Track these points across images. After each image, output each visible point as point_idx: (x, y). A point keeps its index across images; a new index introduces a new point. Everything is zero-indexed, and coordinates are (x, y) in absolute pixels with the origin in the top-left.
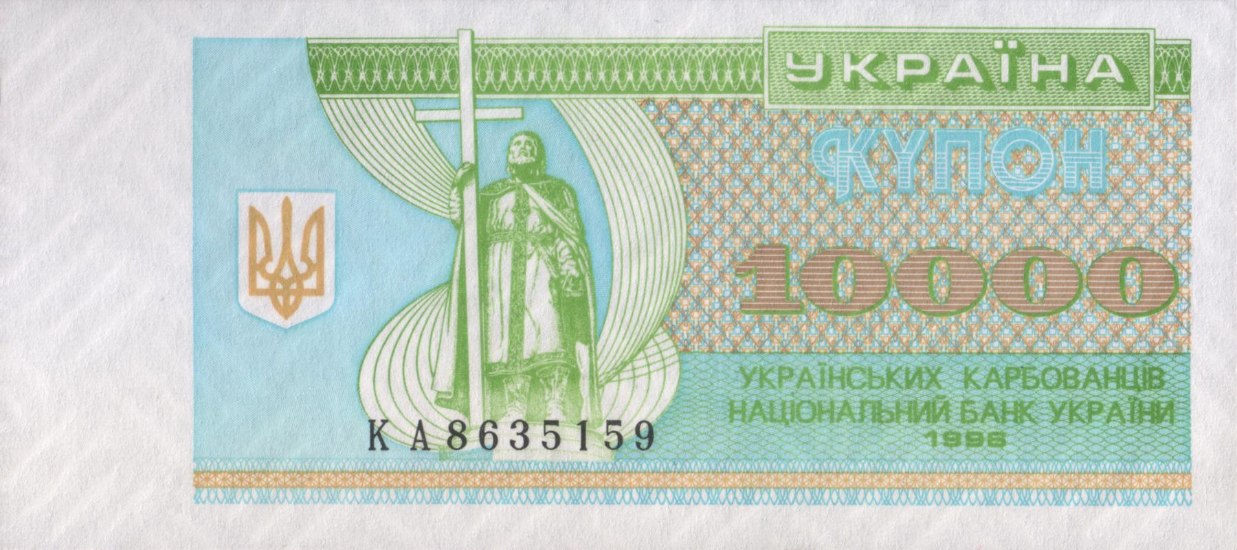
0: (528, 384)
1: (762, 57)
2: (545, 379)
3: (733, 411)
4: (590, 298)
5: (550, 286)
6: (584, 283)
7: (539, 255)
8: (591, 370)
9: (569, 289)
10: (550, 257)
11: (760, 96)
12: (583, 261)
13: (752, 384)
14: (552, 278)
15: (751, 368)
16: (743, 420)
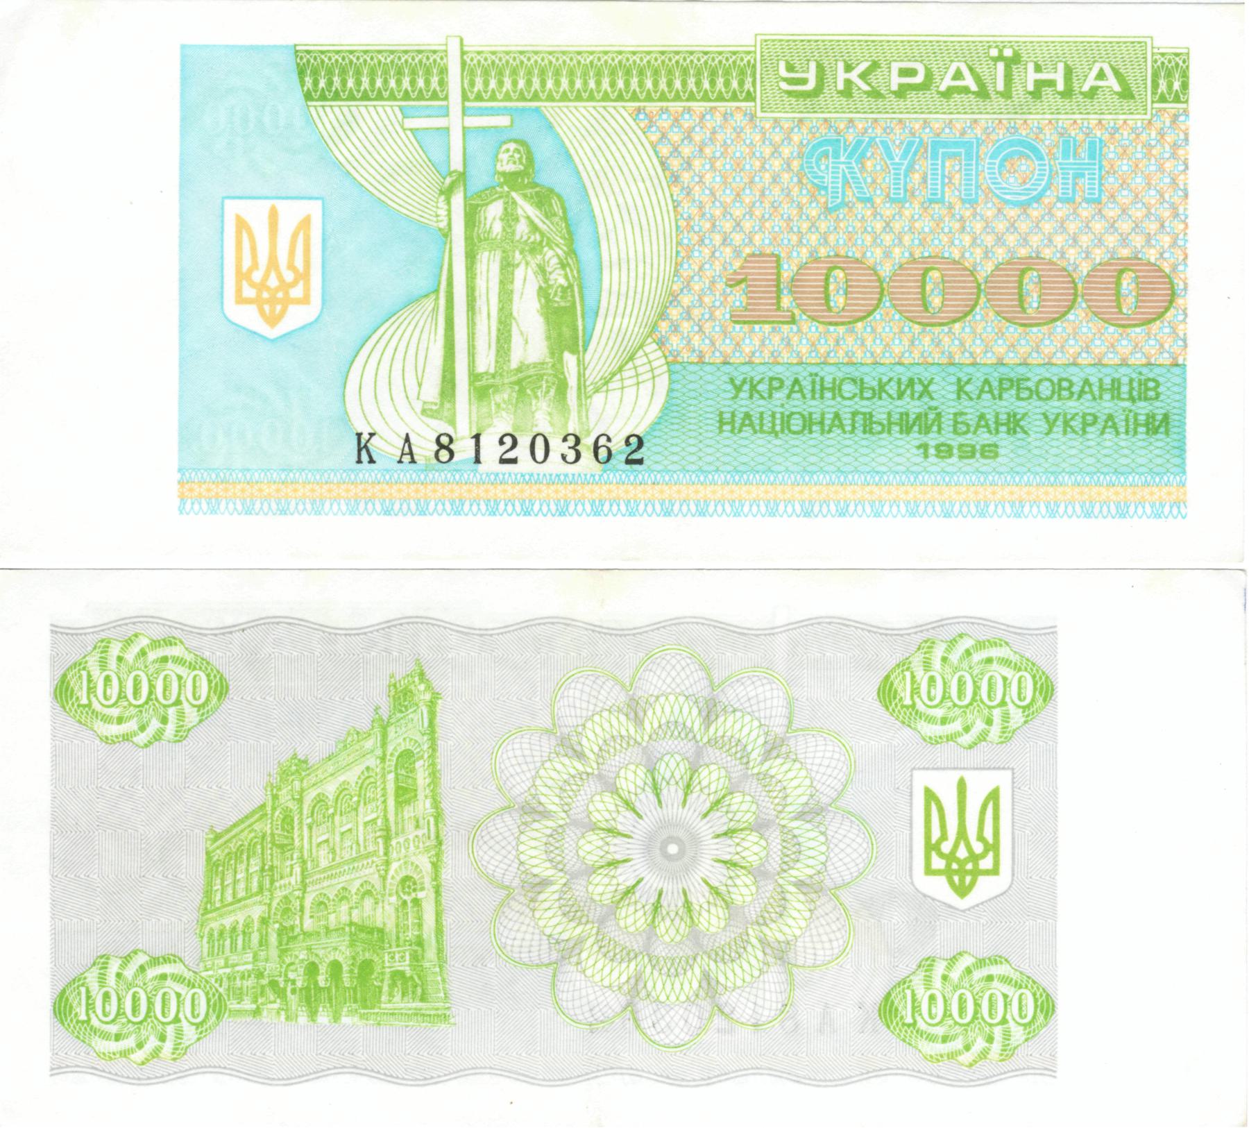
0: (514, 395)
1: (754, 66)
2: (532, 390)
3: (721, 422)
4: (579, 308)
5: (539, 295)
6: (573, 291)
7: (527, 263)
8: (579, 380)
9: (557, 299)
10: (539, 266)
11: (752, 104)
12: (571, 270)
13: (742, 395)
14: (540, 288)
15: (741, 378)
16: (732, 431)
